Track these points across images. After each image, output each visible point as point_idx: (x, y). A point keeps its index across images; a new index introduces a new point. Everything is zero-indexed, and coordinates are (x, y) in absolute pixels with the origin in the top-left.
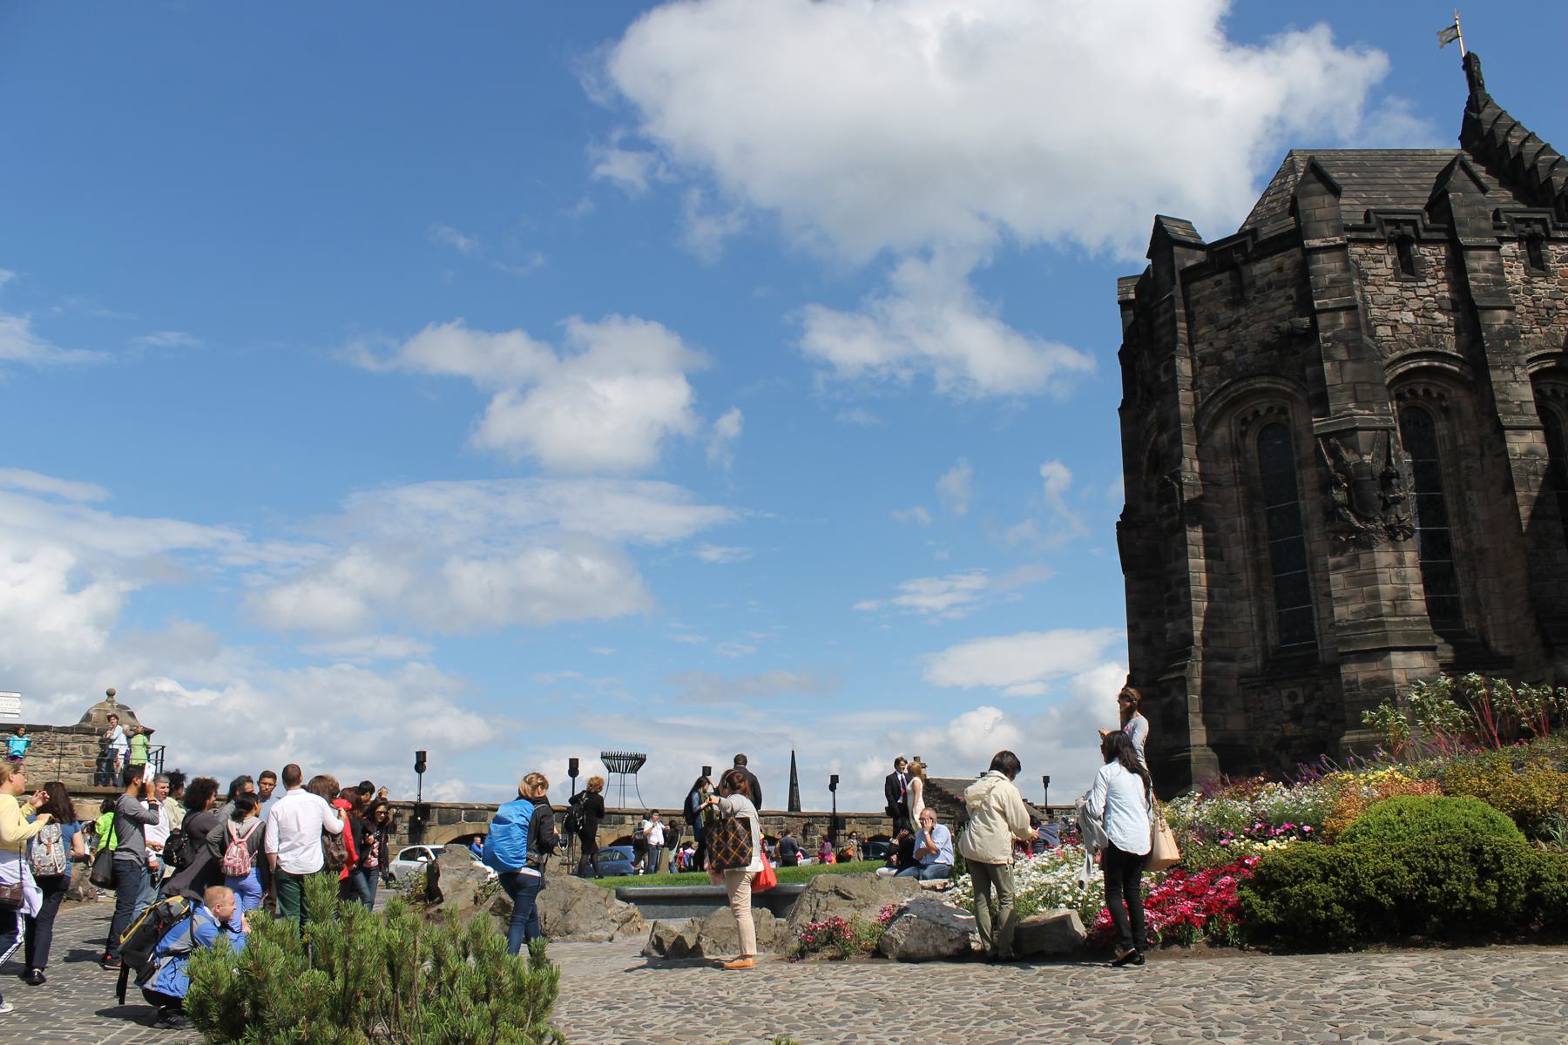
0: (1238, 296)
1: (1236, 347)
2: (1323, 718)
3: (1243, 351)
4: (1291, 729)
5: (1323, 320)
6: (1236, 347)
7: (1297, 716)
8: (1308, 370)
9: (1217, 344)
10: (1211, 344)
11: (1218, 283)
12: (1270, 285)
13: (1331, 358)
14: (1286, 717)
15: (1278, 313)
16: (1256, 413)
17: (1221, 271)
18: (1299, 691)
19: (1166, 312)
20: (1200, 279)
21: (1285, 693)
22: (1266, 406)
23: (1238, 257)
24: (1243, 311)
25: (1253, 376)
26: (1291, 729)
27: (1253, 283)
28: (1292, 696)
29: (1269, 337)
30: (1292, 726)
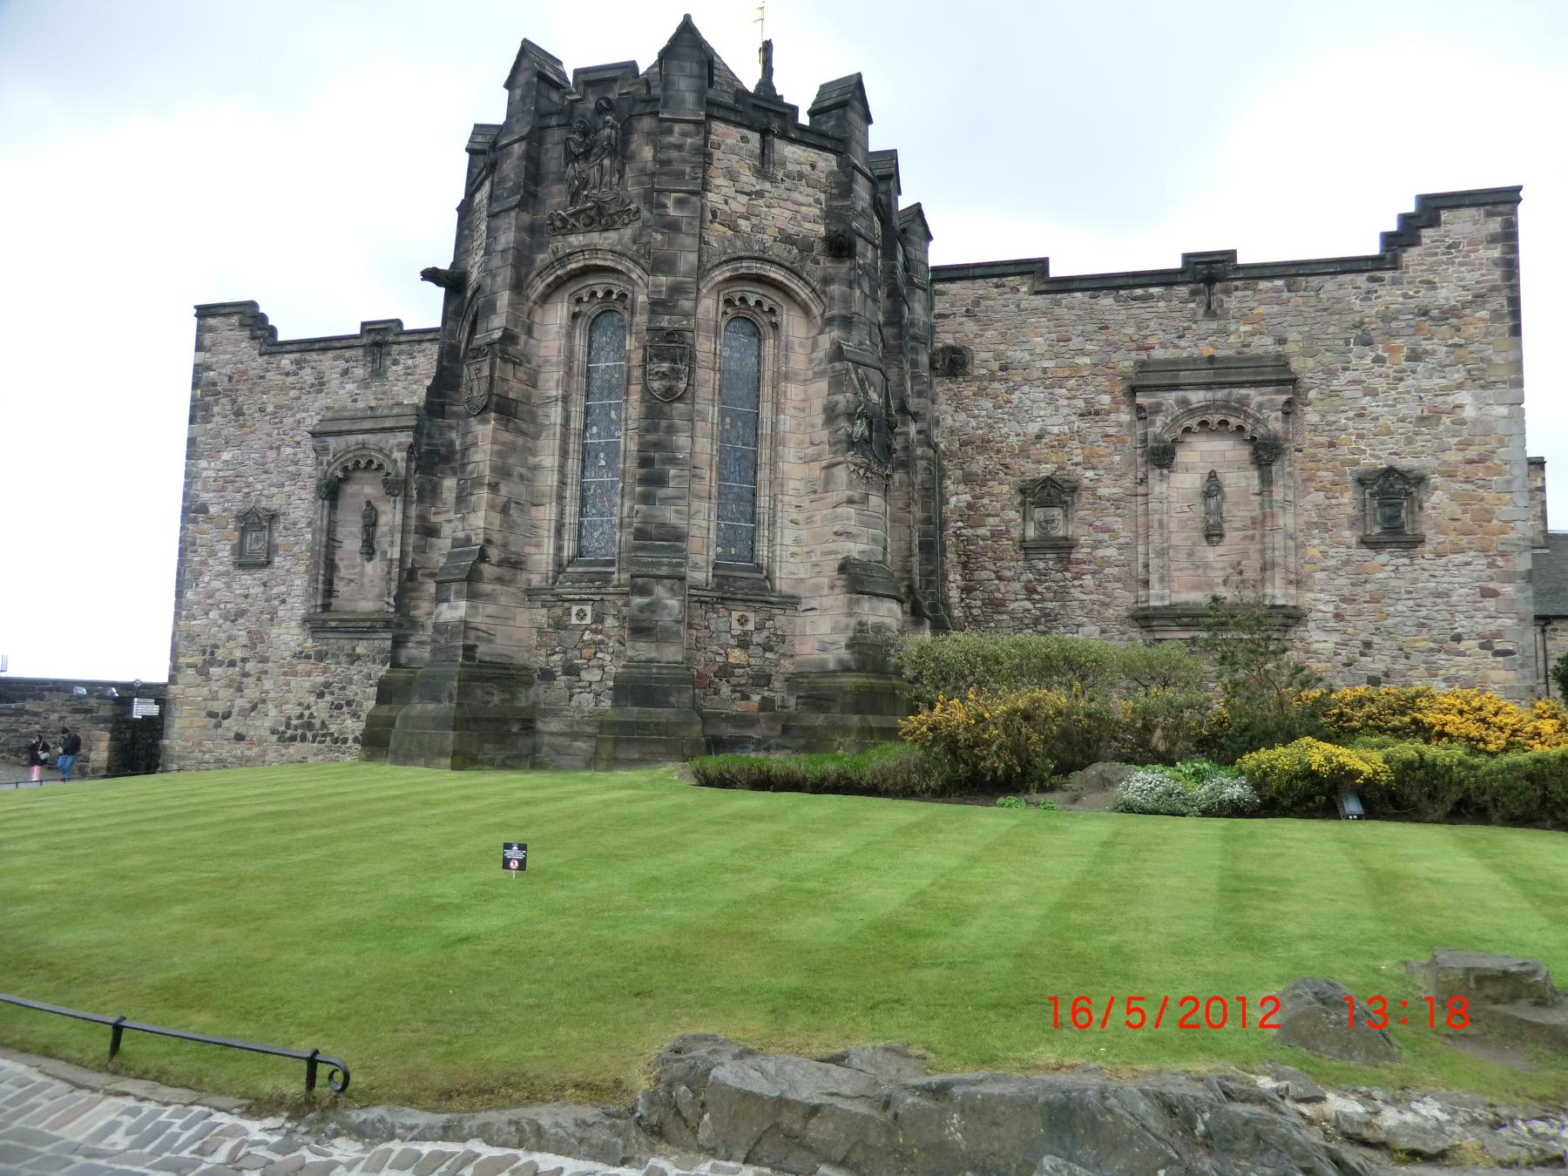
0: (765, 165)
1: (755, 221)
2: (771, 650)
3: (763, 230)
4: (737, 656)
5: (860, 245)
7: (744, 644)
8: (835, 289)
10: (726, 202)
11: (744, 139)
12: (801, 176)
13: (860, 286)
14: (733, 642)
15: (803, 209)
16: (743, 300)
17: (749, 128)
18: (751, 616)
20: (727, 121)
21: (735, 615)
22: (756, 297)
23: (775, 126)
24: (767, 186)
25: (773, 262)
26: (737, 656)
27: (783, 164)
28: (743, 621)
29: (791, 229)
30: (737, 652)
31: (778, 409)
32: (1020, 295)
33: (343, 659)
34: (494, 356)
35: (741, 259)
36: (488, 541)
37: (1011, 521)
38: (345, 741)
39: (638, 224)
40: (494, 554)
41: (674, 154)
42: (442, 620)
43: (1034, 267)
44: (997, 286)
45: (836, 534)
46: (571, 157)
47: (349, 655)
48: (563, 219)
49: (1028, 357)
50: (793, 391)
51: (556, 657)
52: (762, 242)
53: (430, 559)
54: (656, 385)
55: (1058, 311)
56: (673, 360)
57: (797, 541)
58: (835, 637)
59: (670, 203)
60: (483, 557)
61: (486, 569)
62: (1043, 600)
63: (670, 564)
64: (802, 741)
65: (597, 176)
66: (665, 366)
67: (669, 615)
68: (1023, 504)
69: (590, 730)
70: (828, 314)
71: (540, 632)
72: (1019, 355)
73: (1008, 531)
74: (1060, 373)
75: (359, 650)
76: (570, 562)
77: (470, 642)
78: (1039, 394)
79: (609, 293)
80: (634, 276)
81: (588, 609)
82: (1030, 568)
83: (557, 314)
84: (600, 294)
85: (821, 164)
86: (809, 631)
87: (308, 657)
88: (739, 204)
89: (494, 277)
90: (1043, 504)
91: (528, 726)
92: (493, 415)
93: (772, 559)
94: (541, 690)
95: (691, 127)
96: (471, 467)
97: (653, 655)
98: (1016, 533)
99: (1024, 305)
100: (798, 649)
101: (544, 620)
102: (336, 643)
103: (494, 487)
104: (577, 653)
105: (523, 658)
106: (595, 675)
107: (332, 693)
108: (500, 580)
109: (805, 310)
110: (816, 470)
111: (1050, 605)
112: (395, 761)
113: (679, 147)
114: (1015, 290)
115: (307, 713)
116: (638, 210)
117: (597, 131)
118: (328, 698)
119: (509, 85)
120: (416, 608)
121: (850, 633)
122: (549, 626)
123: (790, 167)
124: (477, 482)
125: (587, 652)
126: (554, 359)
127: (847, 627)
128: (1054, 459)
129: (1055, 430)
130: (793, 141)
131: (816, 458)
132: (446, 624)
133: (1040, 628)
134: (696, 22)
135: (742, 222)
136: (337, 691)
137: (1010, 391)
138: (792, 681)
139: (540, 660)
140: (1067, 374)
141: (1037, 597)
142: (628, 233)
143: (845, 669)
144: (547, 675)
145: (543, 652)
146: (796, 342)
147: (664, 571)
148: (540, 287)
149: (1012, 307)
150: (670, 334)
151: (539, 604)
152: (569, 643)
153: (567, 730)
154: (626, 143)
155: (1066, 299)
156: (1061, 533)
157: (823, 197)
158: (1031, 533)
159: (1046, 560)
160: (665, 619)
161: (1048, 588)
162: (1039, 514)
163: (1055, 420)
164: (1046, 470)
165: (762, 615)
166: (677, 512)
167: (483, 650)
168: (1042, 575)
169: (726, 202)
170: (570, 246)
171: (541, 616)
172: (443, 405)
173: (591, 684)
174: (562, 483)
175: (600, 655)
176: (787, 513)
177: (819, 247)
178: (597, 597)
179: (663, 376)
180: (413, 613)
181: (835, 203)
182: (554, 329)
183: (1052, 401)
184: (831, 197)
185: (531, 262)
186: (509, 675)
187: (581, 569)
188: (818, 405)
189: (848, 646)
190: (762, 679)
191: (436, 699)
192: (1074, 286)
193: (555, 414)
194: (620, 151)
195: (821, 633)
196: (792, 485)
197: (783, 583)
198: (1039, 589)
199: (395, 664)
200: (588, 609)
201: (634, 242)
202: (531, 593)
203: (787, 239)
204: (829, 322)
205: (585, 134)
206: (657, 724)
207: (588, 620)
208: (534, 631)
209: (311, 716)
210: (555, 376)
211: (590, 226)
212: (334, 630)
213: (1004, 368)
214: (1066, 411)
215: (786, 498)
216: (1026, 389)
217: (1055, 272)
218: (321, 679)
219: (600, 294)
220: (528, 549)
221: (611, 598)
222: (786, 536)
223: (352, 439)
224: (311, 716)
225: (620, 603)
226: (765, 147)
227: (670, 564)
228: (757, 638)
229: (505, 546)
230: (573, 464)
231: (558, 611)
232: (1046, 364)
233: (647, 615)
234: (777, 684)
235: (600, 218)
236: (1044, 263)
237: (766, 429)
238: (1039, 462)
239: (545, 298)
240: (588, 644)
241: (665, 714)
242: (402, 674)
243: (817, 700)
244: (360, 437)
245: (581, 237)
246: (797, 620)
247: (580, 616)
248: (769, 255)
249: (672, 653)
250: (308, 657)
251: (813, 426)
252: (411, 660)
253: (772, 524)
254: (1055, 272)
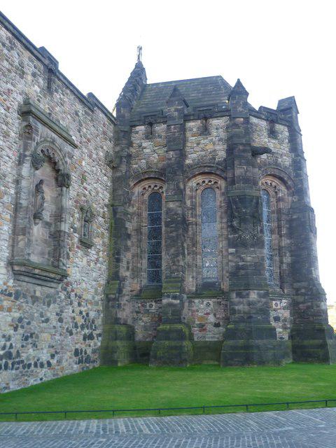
33: (30, 299)
38: (29, 365)
47: (32, 297)
75: (38, 294)
87: (10, 295)
102: (27, 286)
107: (22, 327)
115: (8, 344)
118: (20, 331)
136: (26, 326)
209: (11, 346)
212: (34, 276)
218: (17, 315)
223: (49, 132)
224: (11, 346)
244: (54, 135)
250: (10, 295)
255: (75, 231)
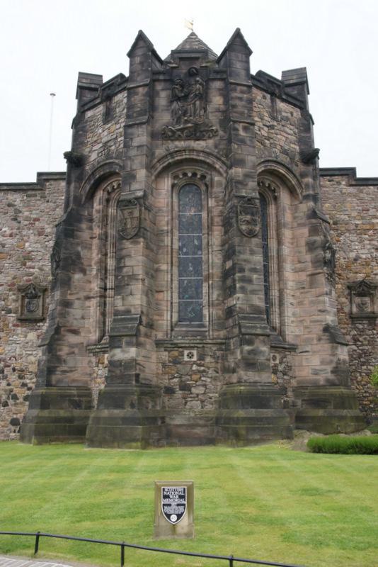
0: (274, 113)
1: (272, 141)
6: (272, 141)
9: (263, 132)
10: (260, 131)
12: (287, 119)
17: (267, 92)
18: (277, 355)
19: (242, 92)
22: (268, 182)
24: (275, 123)
29: (287, 147)
30: (273, 376)
31: (280, 243)
32: (342, 186)
34: (141, 206)
35: (268, 161)
36: (142, 312)
37: (343, 303)
39: (218, 138)
40: (144, 318)
41: (238, 102)
42: (116, 358)
43: (348, 172)
44: (330, 181)
45: (320, 311)
46: (174, 98)
48: (172, 131)
49: (348, 219)
50: (287, 234)
51: (176, 380)
52: (275, 152)
53: (68, 322)
54: (244, 227)
55: (361, 195)
56: (252, 214)
57: (294, 315)
58: (323, 367)
59: (240, 127)
60: (140, 323)
61: (142, 329)
62: (362, 345)
63: (261, 328)
64: (311, 425)
65: (193, 109)
66: (248, 217)
67: (263, 356)
68: (350, 294)
69: (201, 422)
70: (304, 194)
71: (164, 365)
72: (343, 217)
73: (342, 309)
74: (365, 227)
76: (176, 325)
77: (137, 372)
78: (353, 237)
79: (194, 175)
80: (217, 166)
81: (195, 352)
82: (355, 328)
83: (166, 184)
84: (190, 175)
85: (295, 114)
86: (304, 364)
88: (264, 132)
89: (133, 160)
90: (361, 295)
91: (163, 419)
92: (142, 240)
93: (282, 323)
94: (166, 399)
95: (245, 88)
96: (125, 270)
97: (257, 379)
98: (346, 309)
99: (344, 191)
100: (297, 374)
101: (167, 358)
103: (143, 280)
104: (189, 377)
105: (155, 381)
106: (201, 390)
108: (146, 336)
109: (292, 191)
110: (303, 277)
111: (366, 348)
112: (92, 443)
113: (241, 99)
114: (339, 183)
116: (217, 131)
117: (190, 85)
119: (130, 54)
120: (60, 350)
121: (334, 365)
122: (170, 362)
123: (284, 114)
124: (133, 277)
125: (195, 377)
126: (165, 209)
127: (331, 362)
128: (364, 271)
129: (364, 256)
130: (283, 100)
131: (302, 270)
132: (120, 362)
133: (362, 360)
134: (243, 32)
135: (266, 141)
137: (339, 235)
138: (299, 390)
139: (165, 382)
140: (368, 227)
141: (360, 343)
142: (211, 142)
143: (331, 384)
144: (170, 391)
145: (167, 377)
146: (287, 207)
147: (259, 331)
148: (160, 167)
149: (338, 192)
150: (249, 200)
151: (163, 349)
152: (183, 372)
153: (186, 422)
154: (207, 93)
155: (366, 189)
156: (369, 310)
157: (296, 131)
158: (355, 310)
159: (363, 324)
160: (262, 359)
161: (365, 339)
162: (358, 300)
163: (363, 251)
164: (360, 277)
165: (282, 355)
166: (259, 298)
167: (141, 376)
168: (362, 332)
169: (260, 131)
170: (176, 147)
171: (165, 356)
172: (73, 231)
173: (198, 395)
174: (172, 280)
175: (203, 378)
176: (288, 300)
177: (297, 158)
178: (201, 346)
179: (248, 223)
180: (59, 353)
181: (302, 135)
182: (164, 192)
183: (361, 241)
184: (300, 131)
185: (153, 154)
186: (149, 391)
187: (184, 329)
188: (303, 242)
189: (332, 372)
190: (283, 391)
191: (121, 406)
192: (370, 182)
193: (167, 240)
194: (204, 97)
195: (314, 364)
196: (290, 284)
197: (290, 338)
198: (361, 339)
199: (49, 384)
200: (195, 352)
201: (216, 146)
202: (159, 344)
203: (285, 152)
204: (307, 197)
205: (182, 86)
206: (267, 418)
207: (195, 358)
208: (160, 365)
210: (166, 219)
211: (188, 138)
213: (335, 223)
214: (369, 247)
215: (288, 291)
216: (347, 234)
217: (359, 175)
219: (190, 175)
220: (156, 317)
221: (208, 346)
222: (289, 311)
225: (214, 349)
226: (273, 101)
227: (261, 328)
228: (280, 368)
229: (147, 315)
230: (175, 270)
231: (176, 353)
232: (358, 222)
233: (252, 356)
234: (290, 394)
235: (197, 132)
236: (353, 171)
237: (273, 253)
238: (356, 273)
239: (160, 175)
240: (195, 373)
241: (267, 412)
242: (54, 390)
243: (317, 402)
245: (182, 143)
246: (296, 358)
247: (190, 356)
248: (279, 160)
249: (267, 377)
251: (300, 252)
252: (59, 381)
253: (281, 304)
254: (359, 175)
255: (10, 311)
